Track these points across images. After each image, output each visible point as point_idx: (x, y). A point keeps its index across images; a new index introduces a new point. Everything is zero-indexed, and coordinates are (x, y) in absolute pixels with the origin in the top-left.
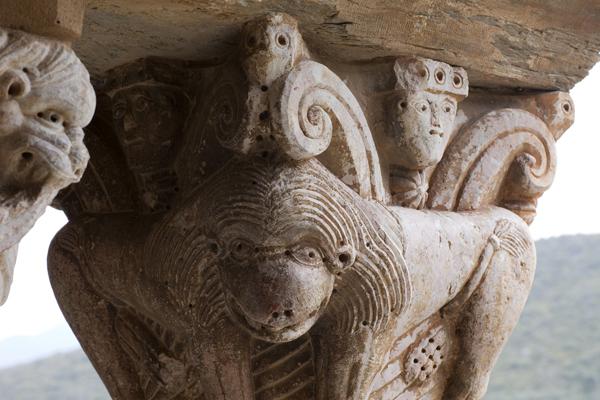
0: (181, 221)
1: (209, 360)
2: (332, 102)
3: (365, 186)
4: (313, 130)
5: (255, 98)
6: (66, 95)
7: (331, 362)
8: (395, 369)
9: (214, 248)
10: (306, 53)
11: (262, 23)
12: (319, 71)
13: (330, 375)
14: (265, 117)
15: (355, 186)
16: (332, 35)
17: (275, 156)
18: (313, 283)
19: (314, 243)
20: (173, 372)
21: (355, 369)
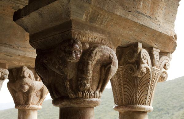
0: (17, 82)
1: (19, 93)
2: (29, 72)
3: (32, 79)
4: (27, 75)
5: (22, 72)
6: (6, 73)
7: (29, 94)
8: (35, 95)
9: (19, 84)
10: (27, 68)
11: (23, 66)
12: (28, 70)
13: (29, 95)
14: (23, 74)
15: (31, 79)
16: (30, 67)
17: (24, 77)
18: (27, 87)
19: (27, 84)
20: (17, 95)
21: (31, 94)
